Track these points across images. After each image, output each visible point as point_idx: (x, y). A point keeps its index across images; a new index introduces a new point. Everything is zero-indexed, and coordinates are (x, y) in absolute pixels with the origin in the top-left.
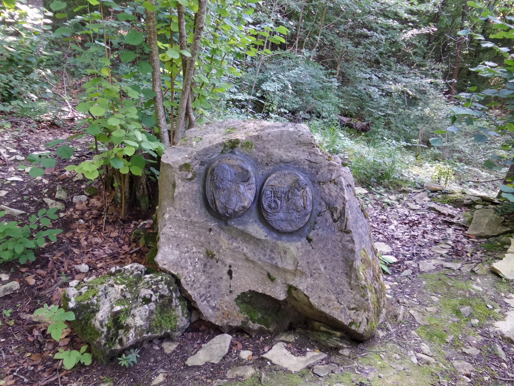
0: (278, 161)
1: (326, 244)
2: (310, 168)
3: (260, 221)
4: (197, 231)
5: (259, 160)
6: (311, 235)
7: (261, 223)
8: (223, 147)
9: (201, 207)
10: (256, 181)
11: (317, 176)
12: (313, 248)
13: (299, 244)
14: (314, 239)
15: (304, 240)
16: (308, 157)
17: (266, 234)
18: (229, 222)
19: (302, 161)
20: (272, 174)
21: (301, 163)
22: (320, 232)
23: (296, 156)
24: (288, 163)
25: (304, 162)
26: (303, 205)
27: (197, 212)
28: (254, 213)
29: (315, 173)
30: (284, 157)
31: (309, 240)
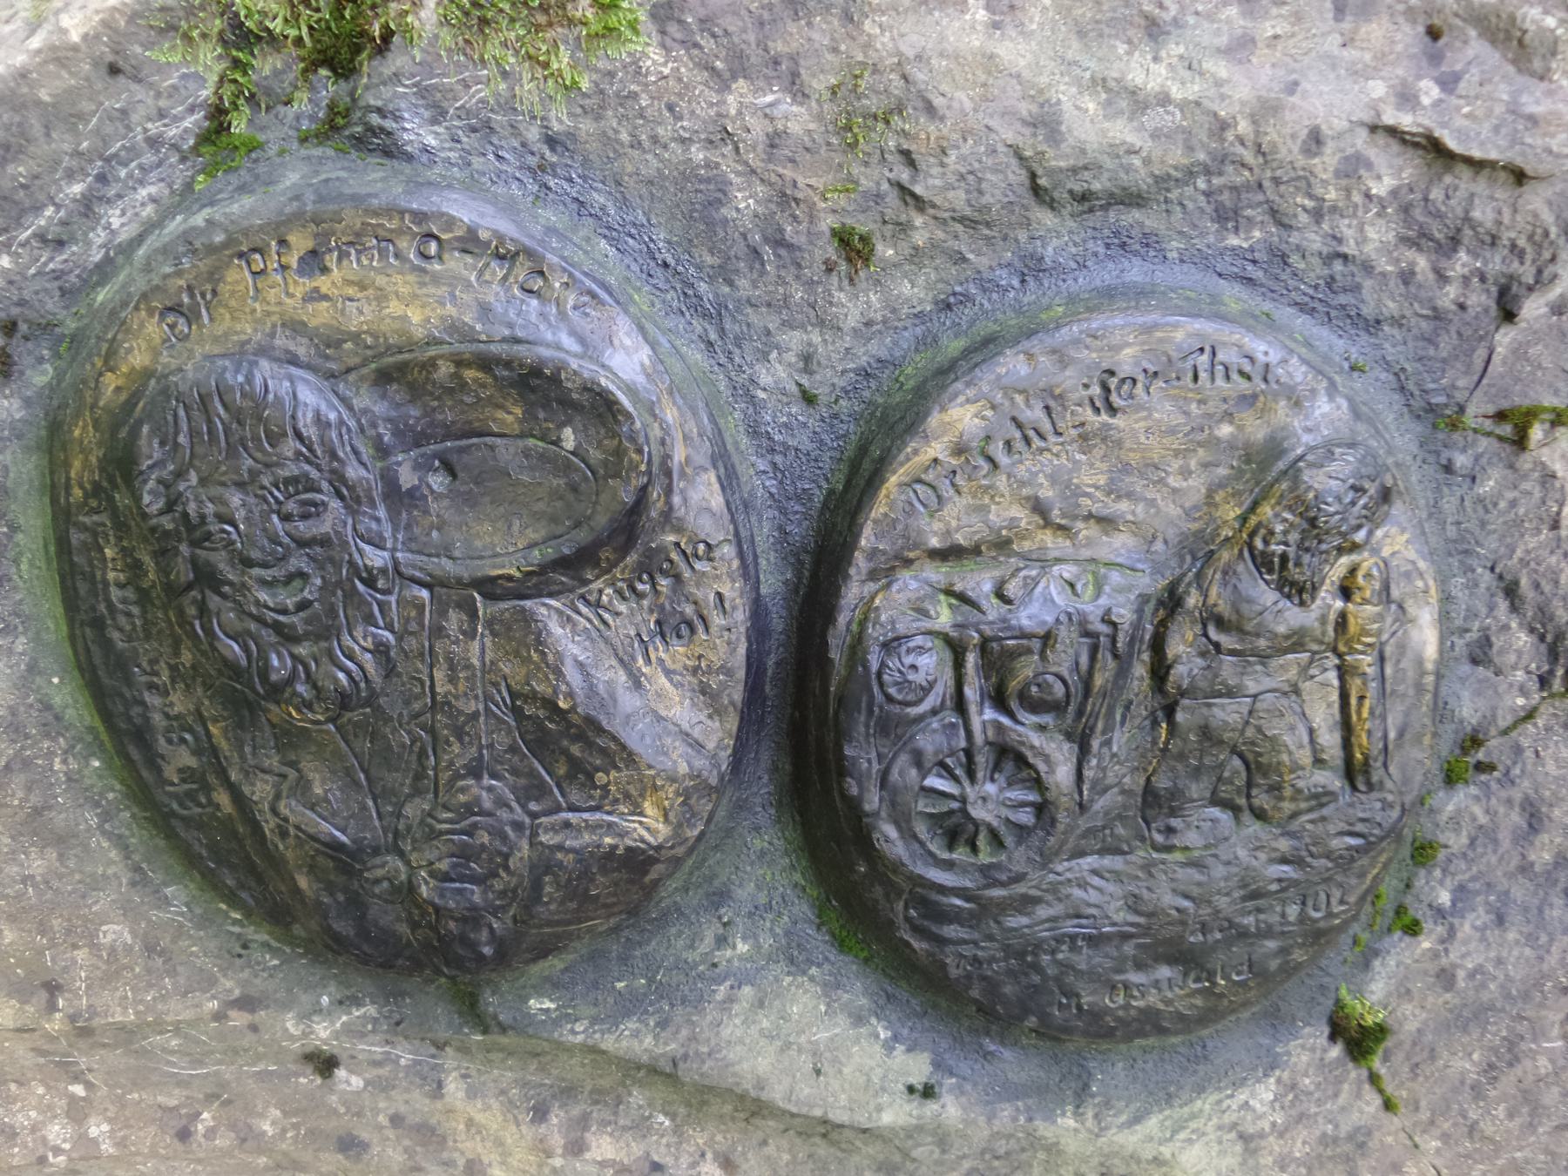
0: (1003, 183)
1: (1512, 1043)
2: (1414, 241)
3: (841, 945)
4: (182, 1083)
5: (745, 202)
6: (1373, 997)
7: (849, 966)
8: (209, 61)
9: (139, 878)
10: (738, 507)
11: (1505, 338)
12: (1388, 1105)
13: (1263, 1094)
14: (1410, 1019)
15: (1310, 1048)
16: (1406, 98)
17: (918, 1068)
18: (490, 1001)
19: (1326, 163)
20: (942, 378)
21: (1305, 182)
22: (1468, 953)
23: (1238, 88)
24: (1132, 199)
25: (1353, 168)
26: (1330, 740)
27: (114, 932)
28: (764, 870)
29: (1481, 300)
30: (1090, 126)
31: (1358, 1040)
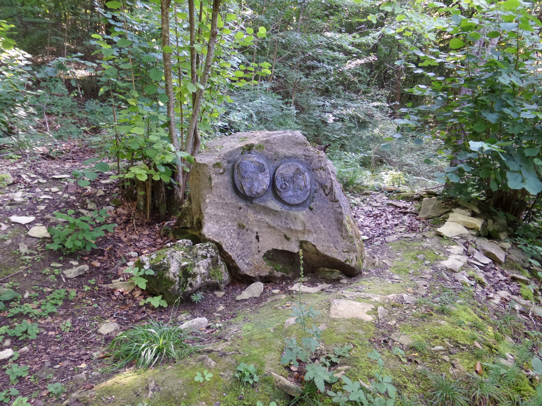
0: (283, 157)
5: (270, 157)
6: (312, 206)
13: (305, 212)
14: (314, 208)
15: (307, 209)
18: (253, 201)
22: (318, 203)
23: (295, 152)
27: (229, 196)
30: (287, 154)
31: (311, 209)
